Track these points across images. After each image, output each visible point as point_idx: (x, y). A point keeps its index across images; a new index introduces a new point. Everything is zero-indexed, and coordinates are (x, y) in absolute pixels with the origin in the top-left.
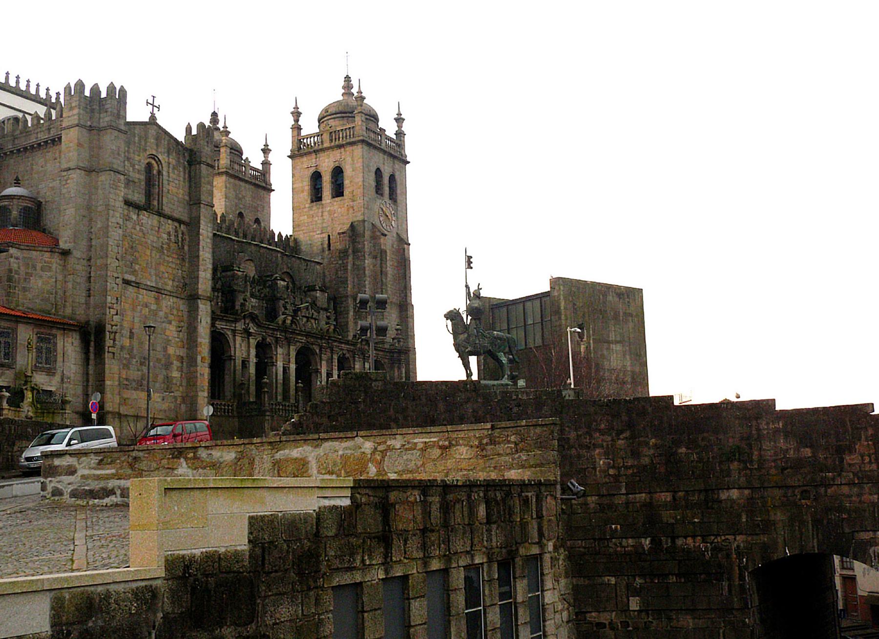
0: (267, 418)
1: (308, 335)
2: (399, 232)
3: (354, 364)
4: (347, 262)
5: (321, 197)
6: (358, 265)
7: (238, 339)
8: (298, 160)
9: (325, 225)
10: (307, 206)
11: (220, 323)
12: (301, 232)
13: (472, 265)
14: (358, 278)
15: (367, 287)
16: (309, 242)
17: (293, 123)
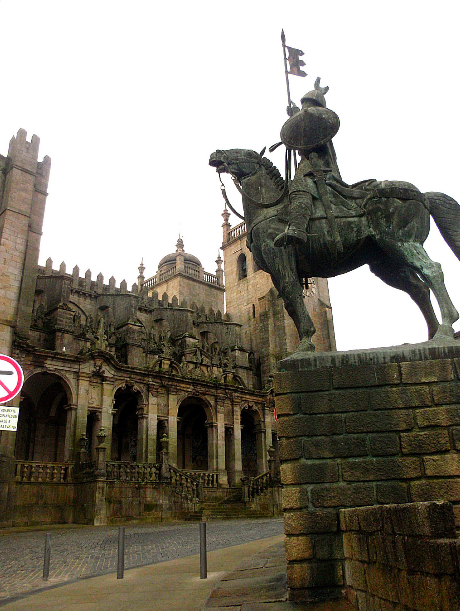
0: (100, 485)
1: (195, 382)
2: (321, 299)
3: (264, 418)
4: (268, 324)
5: (246, 275)
6: (279, 326)
7: (84, 384)
8: (228, 250)
9: (250, 297)
10: (236, 284)
11: (53, 363)
12: (232, 307)
13: (302, 68)
14: (279, 338)
15: (288, 345)
16: (238, 314)
17: (224, 222)
